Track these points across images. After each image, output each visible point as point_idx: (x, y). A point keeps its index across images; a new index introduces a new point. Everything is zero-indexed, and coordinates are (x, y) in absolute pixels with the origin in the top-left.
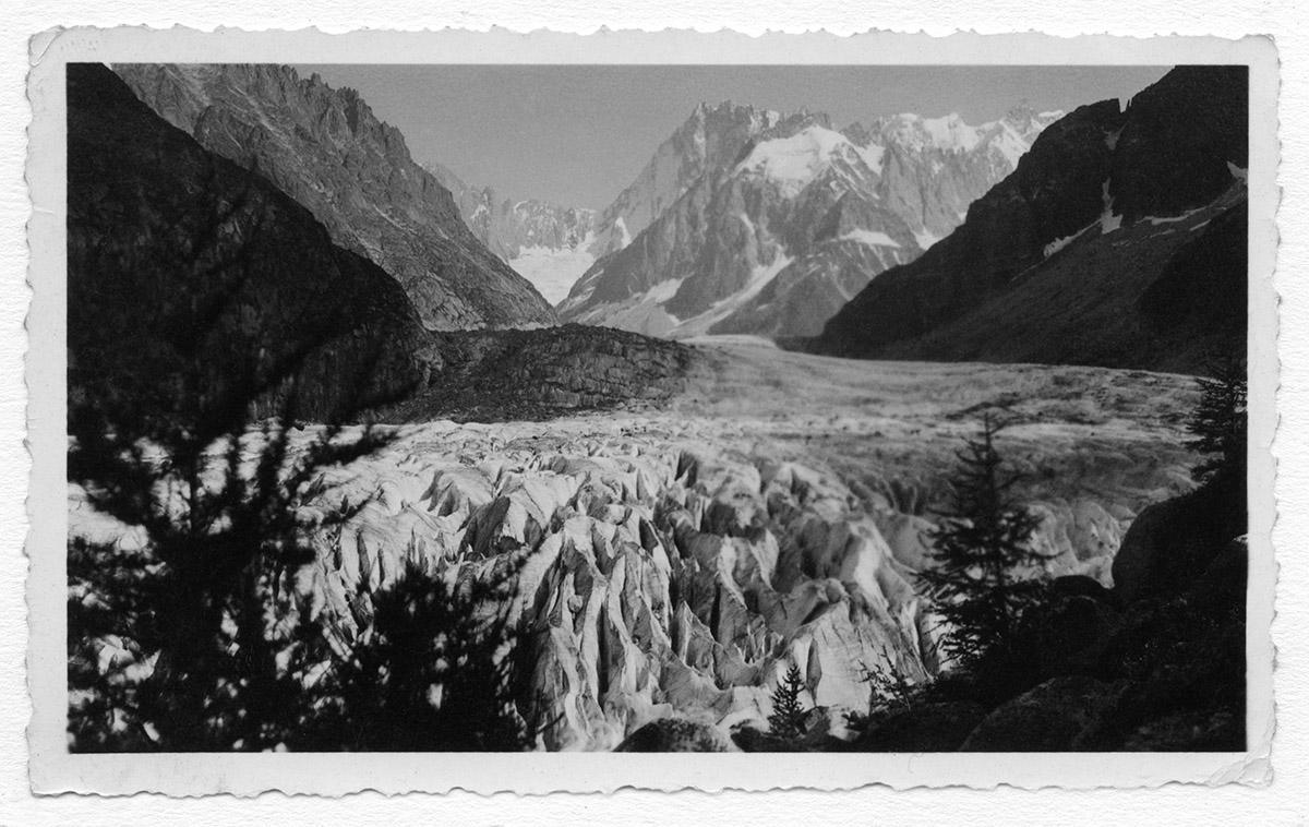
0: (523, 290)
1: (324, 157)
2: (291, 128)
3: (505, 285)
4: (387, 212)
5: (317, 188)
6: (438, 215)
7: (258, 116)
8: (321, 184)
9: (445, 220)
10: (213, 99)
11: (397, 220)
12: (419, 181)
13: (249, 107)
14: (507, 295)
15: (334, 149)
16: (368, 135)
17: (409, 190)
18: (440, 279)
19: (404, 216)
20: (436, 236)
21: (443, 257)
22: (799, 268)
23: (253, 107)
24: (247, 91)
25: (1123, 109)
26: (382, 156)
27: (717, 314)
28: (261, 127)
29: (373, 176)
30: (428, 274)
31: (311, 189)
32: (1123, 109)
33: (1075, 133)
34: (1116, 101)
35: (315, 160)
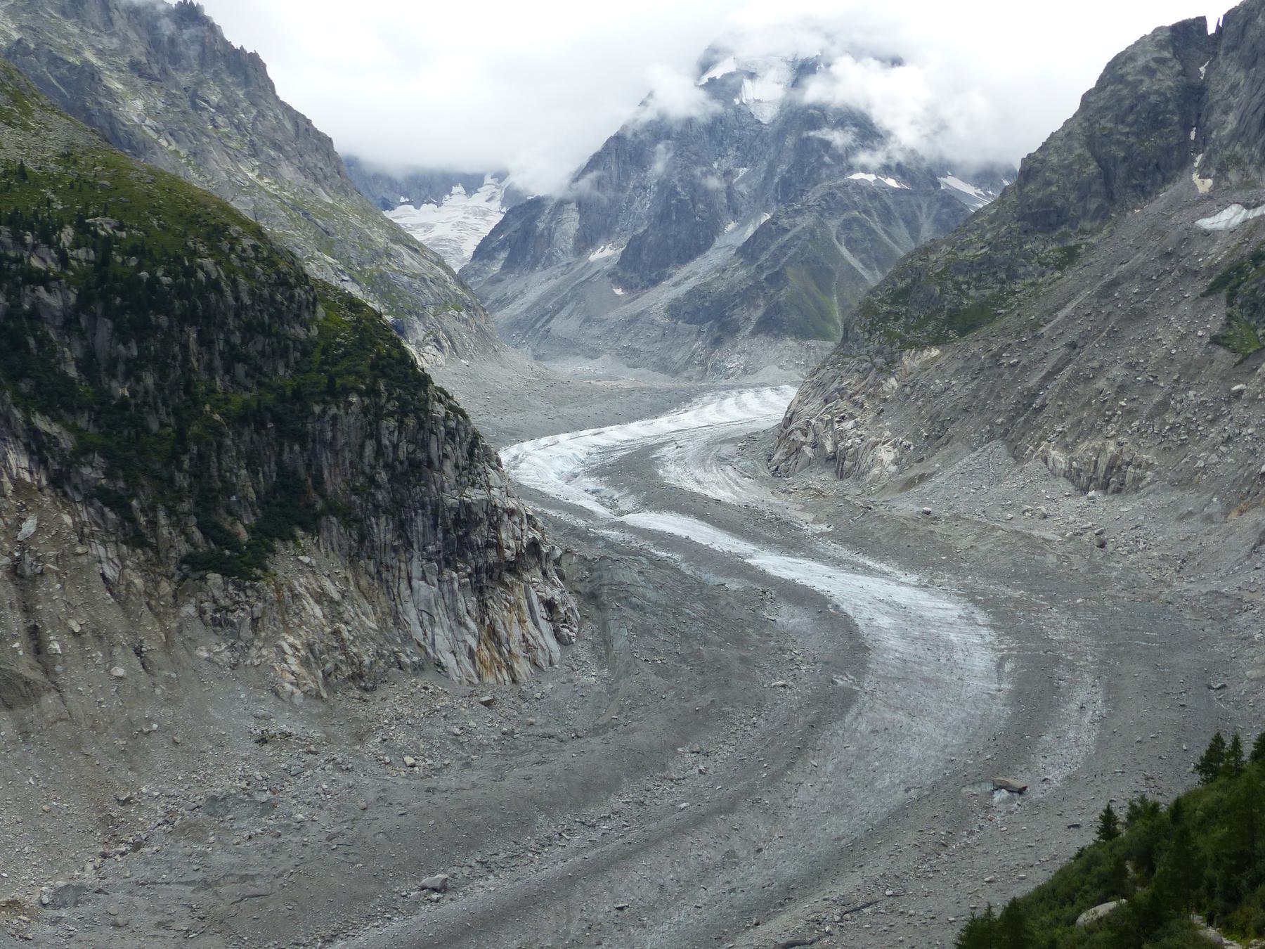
0: (432, 268)
1: (171, 101)
2: (123, 61)
3: (408, 259)
4: (253, 171)
5: (165, 143)
6: (318, 172)
7: (81, 47)
8: (170, 138)
9: (325, 177)
10: (21, 28)
11: (266, 180)
12: (289, 125)
13: (67, 36)
14: (413, 276)
15: (177, 86)
16: (221, 65)
17: (279, 137)
18: (330, 260)
19: (277, 177)
20: (319, 201)
21: (331, 230)
22: (784, 222)
23: (73, 35)
24: (64, 13)
25: (1211, 30)
26: (241, 93)
27: (676, 285)
28: (86, 63)
29: (232, 123)
30: (317, 253)
31: (161, 147)
32: (1211, 30)
33: (1153, 65)
34: (1201, 21)
35: (160, 105)
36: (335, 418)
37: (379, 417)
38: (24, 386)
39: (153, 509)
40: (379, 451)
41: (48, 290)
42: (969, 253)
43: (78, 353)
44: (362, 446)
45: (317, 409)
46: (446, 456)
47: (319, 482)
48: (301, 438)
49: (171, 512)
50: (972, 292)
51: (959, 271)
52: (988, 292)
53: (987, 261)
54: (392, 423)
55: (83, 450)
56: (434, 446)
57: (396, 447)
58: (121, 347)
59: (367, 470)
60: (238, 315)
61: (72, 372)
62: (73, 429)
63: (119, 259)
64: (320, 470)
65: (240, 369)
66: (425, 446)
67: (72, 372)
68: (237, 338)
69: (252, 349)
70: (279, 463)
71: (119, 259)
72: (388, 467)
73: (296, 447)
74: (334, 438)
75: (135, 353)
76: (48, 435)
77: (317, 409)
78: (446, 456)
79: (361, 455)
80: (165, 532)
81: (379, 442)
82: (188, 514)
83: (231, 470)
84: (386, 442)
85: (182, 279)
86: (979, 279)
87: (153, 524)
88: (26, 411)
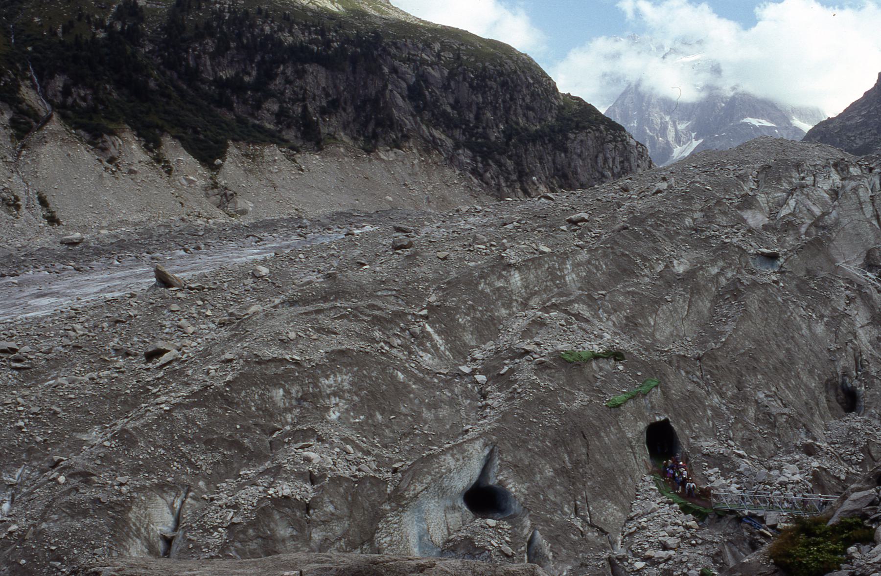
36: (582, 141)
37: (602, 144)
38: (427, 115)
39: (497, 177)
40: (605, 160)
41: (433, 69)
42: (853, 122)
43: (451, 101)
44: (597, 157)
45: (571, 136)
46: (638, 166)
47: (575, 173)
48: (565, 151)
49: (507, 180)
50: (858, 141)
51: (849, 130)
52: (867, 141)
53: (864, 124)
54: (611, 146)
55: (457, 146)
56: (632, 160)
57: (614, 159)
58: (474, 97)
59: (600, 170)
60: (527, 87)
61: (449, 109)
62: (452, 137)
63: (465, 58)
64: (576, 166)
65: (531, 114)
66: (628, 159)
67: (449, 109)
68: (528, 99)
69: (536, 105)
70: (554, 163)
71: (465, 58)
72: (611, 170)
73: (563, 155)
74: (582, 152)
75: (481, 100)
76: (440, 139)
77: (571, 136)
78: (638, 166)
79: (596, 162)
80: (505, 189)
81: (605, 155)
82: (515, 181)
83: (532, 163)
84: (608, 156)
85: (498, 68)
86: (861, 134)
87: (498, 185)
88: (428, 127)
